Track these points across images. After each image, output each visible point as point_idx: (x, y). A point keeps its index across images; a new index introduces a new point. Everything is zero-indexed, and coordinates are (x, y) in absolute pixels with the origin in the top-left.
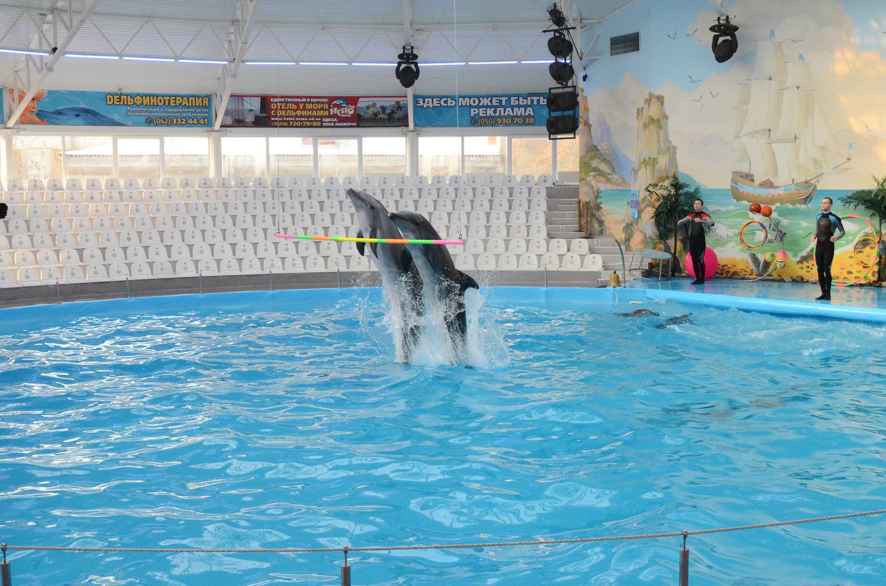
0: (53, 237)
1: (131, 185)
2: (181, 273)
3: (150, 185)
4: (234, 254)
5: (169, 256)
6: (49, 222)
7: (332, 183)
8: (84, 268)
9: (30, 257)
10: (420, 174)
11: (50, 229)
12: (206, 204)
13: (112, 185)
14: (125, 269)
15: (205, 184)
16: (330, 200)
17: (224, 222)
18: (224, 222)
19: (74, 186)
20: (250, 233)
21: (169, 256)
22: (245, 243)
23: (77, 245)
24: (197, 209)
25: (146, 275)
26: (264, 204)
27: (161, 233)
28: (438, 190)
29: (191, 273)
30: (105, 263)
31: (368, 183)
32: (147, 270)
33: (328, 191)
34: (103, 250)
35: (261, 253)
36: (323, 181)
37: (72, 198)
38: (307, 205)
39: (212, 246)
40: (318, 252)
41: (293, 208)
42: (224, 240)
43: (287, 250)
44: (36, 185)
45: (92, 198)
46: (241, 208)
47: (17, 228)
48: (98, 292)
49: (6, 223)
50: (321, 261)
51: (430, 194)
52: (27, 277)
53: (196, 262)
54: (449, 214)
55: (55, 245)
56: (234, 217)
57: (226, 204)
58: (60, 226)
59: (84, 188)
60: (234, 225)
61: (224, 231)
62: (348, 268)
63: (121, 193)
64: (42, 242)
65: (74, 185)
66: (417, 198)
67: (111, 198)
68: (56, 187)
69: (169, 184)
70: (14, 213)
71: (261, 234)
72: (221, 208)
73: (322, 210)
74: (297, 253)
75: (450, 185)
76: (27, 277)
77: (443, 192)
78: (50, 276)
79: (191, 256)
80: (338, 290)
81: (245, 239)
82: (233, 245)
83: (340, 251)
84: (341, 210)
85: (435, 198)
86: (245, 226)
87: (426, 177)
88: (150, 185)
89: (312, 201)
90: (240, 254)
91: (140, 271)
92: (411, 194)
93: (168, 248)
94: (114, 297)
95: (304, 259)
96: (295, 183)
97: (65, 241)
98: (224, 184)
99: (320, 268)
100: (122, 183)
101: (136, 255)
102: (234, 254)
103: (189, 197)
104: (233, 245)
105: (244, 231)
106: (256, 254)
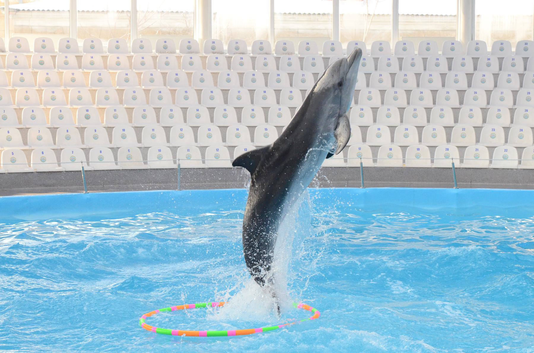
1: (92, 47)
2: (154, 164)
3: (117, 47)
4: (224, 140)
5: (139, 141)
8: (28, 152)
10: (476, 39)
12: (189, 75)
13: (68, 47)
14: (81, 156)
15: (189, 48)
17: (212, 98)
18: (212, 98)
19: (19, 46)
20: (245, 114)
21: (139, 141)
22: (239, 126)
23: (20, 123)
24: (177, 80)
25: (108, 164)
26: (266, 75)
27: (130, 110)
28: (501, 59)
29: (167, 163)
30: (55, 147)
31: (405, 49)
32: (109, 156)
34: (53, 130)
37: (16, 63)
39: (195, 129)
42: (212, 121)
45: (42, 63)
46: (235, 78)
48: (46, 186)
51: (488, 65)
53: (174, 150)
54: (515, 93)
56: (225, 92)
57: (215, 75)
59: (32, 49)
60: (226, 102)
61: (211, 110)
62: (375, 161)
63: (79, 58)
65: (19, 46)
66: (471, 70)
67: (66, 63)
69: (142, 47)
72: (209, 79)
75: (517, 53)
77: (507, 63)
79: (168, 141)
80: (361, 190)
81: (239, 120)
82: (223, 129)
83: (364, 140)
84: (368, 85)
85: (496, 70)
87: (484, 43)
88: (117, 47)
91: (101, 159)
93: (138, 130)
94: (65, 191)
96: (308, 49)
98: (213, 48)
100: (81, 43)
101: (96, 137)
102: (224, 140)
103: (167, 64)
104: (223, 129)
105: (239, 110)
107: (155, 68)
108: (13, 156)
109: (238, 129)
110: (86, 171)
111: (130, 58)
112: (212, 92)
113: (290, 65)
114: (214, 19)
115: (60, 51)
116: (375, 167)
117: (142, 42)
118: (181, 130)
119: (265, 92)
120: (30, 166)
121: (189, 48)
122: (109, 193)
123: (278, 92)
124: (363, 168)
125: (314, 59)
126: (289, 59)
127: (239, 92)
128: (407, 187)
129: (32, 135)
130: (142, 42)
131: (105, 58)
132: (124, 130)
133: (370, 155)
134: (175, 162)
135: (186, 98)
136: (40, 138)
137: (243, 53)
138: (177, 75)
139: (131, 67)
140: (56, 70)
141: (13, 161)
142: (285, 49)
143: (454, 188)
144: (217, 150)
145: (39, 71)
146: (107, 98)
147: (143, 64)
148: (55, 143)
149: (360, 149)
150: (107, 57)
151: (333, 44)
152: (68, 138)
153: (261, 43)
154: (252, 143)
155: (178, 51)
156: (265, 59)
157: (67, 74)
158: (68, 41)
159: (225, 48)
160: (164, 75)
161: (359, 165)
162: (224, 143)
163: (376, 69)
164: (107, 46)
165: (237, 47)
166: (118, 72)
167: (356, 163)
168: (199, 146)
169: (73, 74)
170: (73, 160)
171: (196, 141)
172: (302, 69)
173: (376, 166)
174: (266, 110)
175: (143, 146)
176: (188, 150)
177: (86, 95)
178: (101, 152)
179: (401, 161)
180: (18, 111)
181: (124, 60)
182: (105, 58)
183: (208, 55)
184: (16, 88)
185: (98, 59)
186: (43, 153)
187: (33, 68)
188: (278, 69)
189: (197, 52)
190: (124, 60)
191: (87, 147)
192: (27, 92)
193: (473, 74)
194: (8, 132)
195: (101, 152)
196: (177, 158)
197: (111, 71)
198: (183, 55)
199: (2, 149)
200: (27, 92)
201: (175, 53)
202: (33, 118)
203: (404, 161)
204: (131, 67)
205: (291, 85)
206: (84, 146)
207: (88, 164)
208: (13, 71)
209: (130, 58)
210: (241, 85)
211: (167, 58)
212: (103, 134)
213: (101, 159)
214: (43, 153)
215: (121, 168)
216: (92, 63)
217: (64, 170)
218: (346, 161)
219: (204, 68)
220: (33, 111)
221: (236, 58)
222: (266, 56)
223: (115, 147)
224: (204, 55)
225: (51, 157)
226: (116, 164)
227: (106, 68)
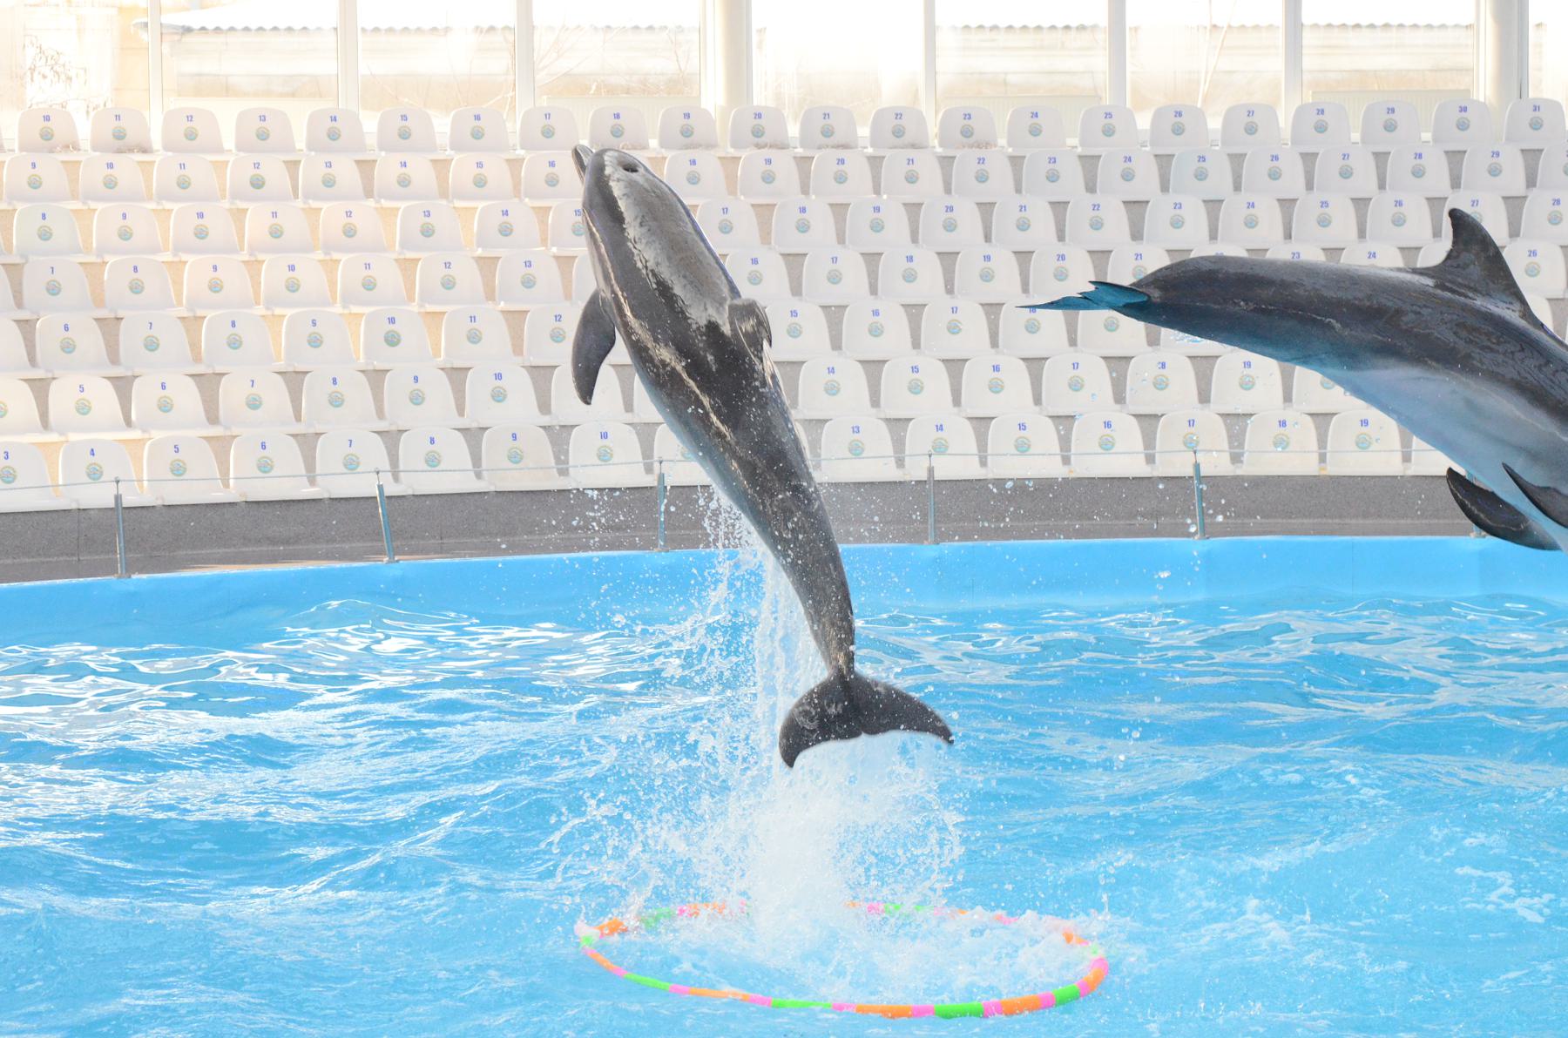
0: (110, 327)
1: (405, 135)
3: (477, 134)
6: (93, 270)
7: (1178, 130)
8: (221, 446)
10: (1531, 95)
11: (99, 302)
13: (334, 135)
14: (376, 454)
16: (1173, 197)
19: (191, 135)
20: (853, 325)
23: (197, 359)
25: (454, 477)
26: (913, 209)
27: (515, 319)
30: (300, 428)
31: (1321, 128)
32: (456, 451)
33: (1164, 161)
34: (294, 380)
35: (897, 401)
36: (1144, 121)
37: (184, 184)
38: (1078, 215)
40: (1119, 398)
41: (1023, 226)
43: (996, 387)
45: (257, 183)
46: (822, 222)
48: (273, 541)
50: (1129, 434)
55: (114, 359)
56: (794, 261)
57: (764, 212)
58: (136, 288)
59: (229, 142)
60: (796, 290)
62: (1236, 459)
63: (365, 166)
64: (68, 347)
65: (190, 136)
66: (1518, 186)
67: (329, 182)
68: (122, 142)
71: (897, 326)
73: (1137, 235)
74: (1037, 400)
78: (95, 474)
81: (836, 345)
83: (1204, 397)
86: (834, 296)
88: (477, 134)
89: (1097, 198)
91: (433, 461)
92: (1494, 171)
94: (329, 556)
95: (1064, 422)
96: (1035, 131)
97: (152, 345)
98: (758, 132)
99: (1127, 462)
100: (370, 124)
101: (417, 399)
105: (834, 314)
106: (875, 402)
108: (177, 456)
110: (389, 498)
111: (515, 164)
112: (755, 261)
113: (982, 178)
114: (760, 47)
115: (311, 146)
116: (1236, 478)
117: (548, 116)
119: (910, 259)
120: (227, 485)
121: (687, 132)
122: (457, 560)
123: (948, 259)
124: (1201, 479)
125: (1053, 160)
126: (981, 161)
127: (835, 260)
128: (1332, 533)
129: (232, 394)
130: (548, 116)
131: (441, 165)
132: (499, 376)
133: (1225, 446)
134: (649, 469)
136: (254, 404)
137: (845, 146)
139: (517, 191)
140: (299, 203)
141: (178, 470)
142: (967, 133)
143: (1472, 535)
145: (251, 206)
146: (448, 284)
148: (298, 418)
149: (1191, 423)
150: (446, 163)
151: (1108, 115)
152: (336, 401)
153: (898, 116)
154: (874, 411)
157: (331, 213)
158: (334, 119)
159: (793, 130)
161: (1188, 471)
163: (1237, 187)
164: (448, 130)
165: (827, 130)
166: (481, 205)
167: (1180, 466)
169: (349, 214)
170: (351, 465)
172: (1018, 190)
173: (1239, 472)
174: (914, 312)
177: (387, 274)
178: (432, 441)
179: (1315, 457)
180: (192, 323)
181: (496, 171)
182: (441, 165)
183: (744, 154)
184: (184, 257)
185: (421, 170)
186: (264, 446)
187: (235, 196)
188: (948, 191)
189: (711, 146)
190: (496, 171)
191: (394, 428)
192: (215, 268)
193: (1525, 197)
194: (163, 386)
195: (432, 441)
197: (459, 204)
198: (669, 154)
200: (215, 268)
202: (235, 343)
203: (1322, 459)
205: (988, 238)
206: (383, 426)
207: (396, 479)
208: (175, 207)
209: (515, 164)
210: (841, 239)
212: (439, 390)
213: (433, 461)
214: (264, 446)
215: (492, 489)
216: (404, 182)
217: (326, 496)
218: (1150, 459)
219: (732, 191)
221: (824, 162)
222: (911, 153)
223: (475, 425)
224: (732, 152)
225: (289, 458)
226: (479, 476)
227: (444, 194)
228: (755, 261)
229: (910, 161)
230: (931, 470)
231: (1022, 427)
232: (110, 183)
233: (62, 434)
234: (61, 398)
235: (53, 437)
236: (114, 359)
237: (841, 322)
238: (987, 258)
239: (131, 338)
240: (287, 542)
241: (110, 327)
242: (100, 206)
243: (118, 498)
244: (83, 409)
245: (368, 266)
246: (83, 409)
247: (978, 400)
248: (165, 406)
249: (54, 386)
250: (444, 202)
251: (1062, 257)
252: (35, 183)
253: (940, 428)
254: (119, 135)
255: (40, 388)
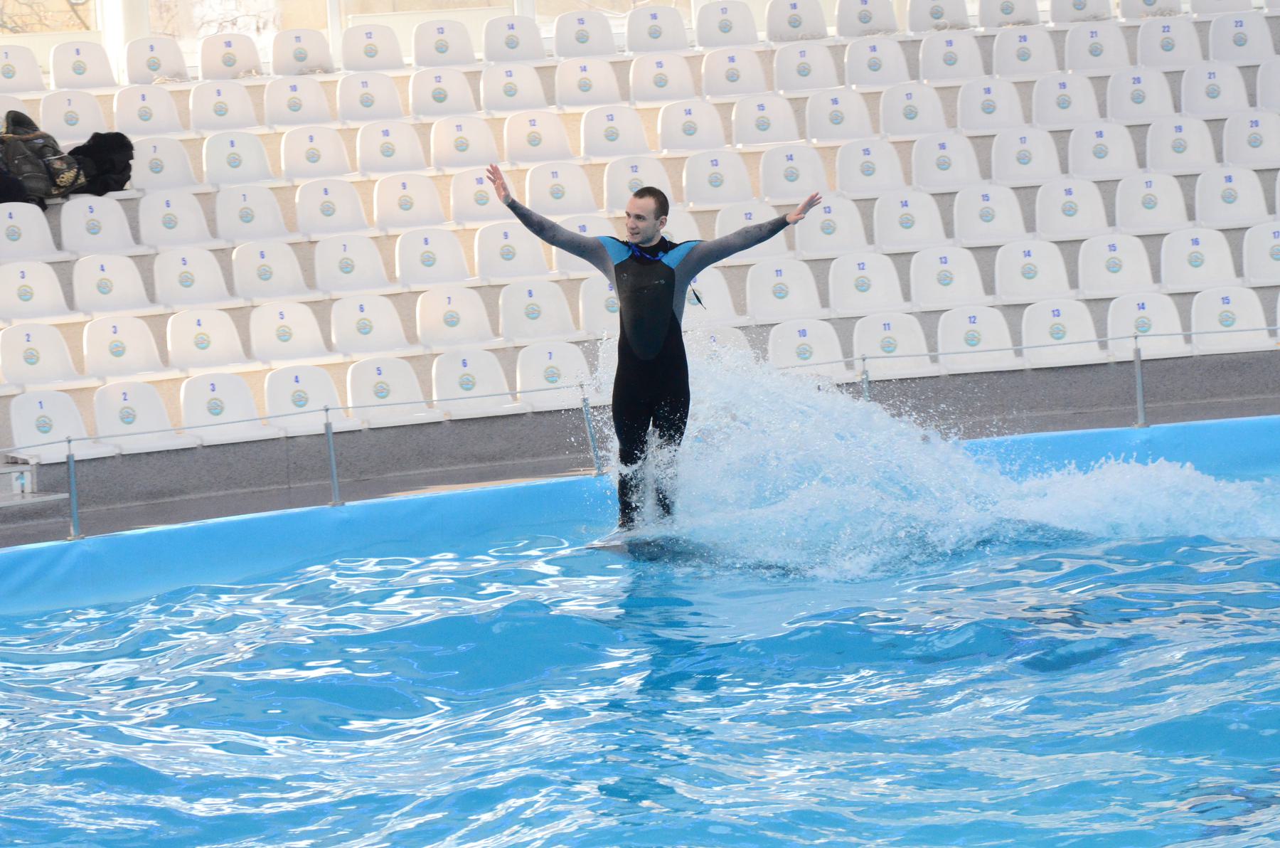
0: (305, 251)
3: (655, 34)
4: (989, 288)
5: (741, 308)
6: (284, 195)
8: (421, 364)
9: (223, 333)
11: (292, 226)
12: (872, 99)
13: (512, 44)
17: (944, 165)
18: (944, 165)
19: (371, 52)
21: (741, 308)
22: (1029, 242)
23: (392, 278)
24: (837, 119)
26: (1100, 83)
30: (499, 343)
34: (489, 293)
35: (1095, 282)
39: (902, 259)
41: (1213, 93)
42: (949, 233)
43: (1196, 261)
44: (230, 62)
45: (440, 97)
47: (170, 223)
48: (480, 459)
49: (131, 207)
52: (215, 408)
55: (311, 283)
56: (982, 143)
57: (948, 94)
58: (328, 210)
59: (409, 59)
60: (986, 173)
61: (945, 199)
63: (546, 73)
64: (265, 274)
65: (371, 54)
67: (510, 91)
68: (303, 63)
69: (725, 28)
70: (156, 168)
71: (1091, 203)
74: (1239, 272)
76: (215, 408)
79: (825, 303)
81: (1030, 226)
82: (985, 254)
88: (655, 34)
90: (1011, 287)
97: (347, 267)
100: (548, 31)
102: (989, 288)
103: (804, 71)
104: (985, 254)
105: (1026, 194)
106: (1074, 283)
107: (771, 87)
109: (1028, 254)
111: (694, 61)
112: (942, 146)
113: (1168, 46)
115: (490, 57)
118: (861, 266)
119: (1100, 134)
120: (430, 404)
123: (1139, 131)
125: (1239, 24)
126: (1166, 29)
127: (1023, 140)
129: (426, 312)
131: (621, 67)
134: (850, 366)
135: (868, 170)
136: (452, 321)
138: (835, 101)
140: (482, 115)
141: (382, 392)
144: (973, 320)
147: (733, 77)
150: (627, 63)
152: (533, 314)
154: (1073, 292)
155: (832, 30)
156: (1093, 34)
160: (798, 104)
162: (990, 299)
164: (625, 30)
166: (663, 105)
168: (916, 310)
169: (533, 122)
170: (552, 376)
171: (907, 296)
172: (1206, 57)
174: (1107, 188)
175: (752, 323)
176: (887, 326)
180: (384, 243)
181: (676, 69)
182: (621, 67)
184: (373, 176)
185: (601, 74)
188: (1133, 61)
189: (889, 30)
190: (676, 69)
192: (404, 186)
194: (362, 309)
196: (857, 354)
198: (850, 42)
199: (348, 359)
200: (404, 186)
201: (823, 36)
202: (428, 261)
204: (698, 92)
205: (1177, 108)
206: (581, 335)
208: (362, 126)
209: (694, 61)
210: (1028, 119)
211: (803, 53)
216: (585, 86)
217: (529, 410)
219: (914, 75)
220: (426, 241)
221: (1006, 38)
224: (911, 35)
225: (489, 373)
227: (625, 95)
228: (942, 146)
229: (1093, 34)
230: (1138, 352)
231: (1226, 300)
232: (295, 106)
233: (265, 362)
234: (262, 326)
235: (256, 366)
236: (311, 283)
237: (1034, 202)
238: (1179, 129)
239: (325, 262)
240: (493, 458)
241: (305, 251)
242: (287, 130)
243: (328, 426)
244: (284, 335)
245: (555, 174)
246: (284, 335)
247: (1179, 276)
248: (364, 328)
249: (254, 315)
250: (626, 105)
251: (1255, 123)
252: (221, 111)
253: (1142, 307)
254: (301, 57)
255: (241, 317)
